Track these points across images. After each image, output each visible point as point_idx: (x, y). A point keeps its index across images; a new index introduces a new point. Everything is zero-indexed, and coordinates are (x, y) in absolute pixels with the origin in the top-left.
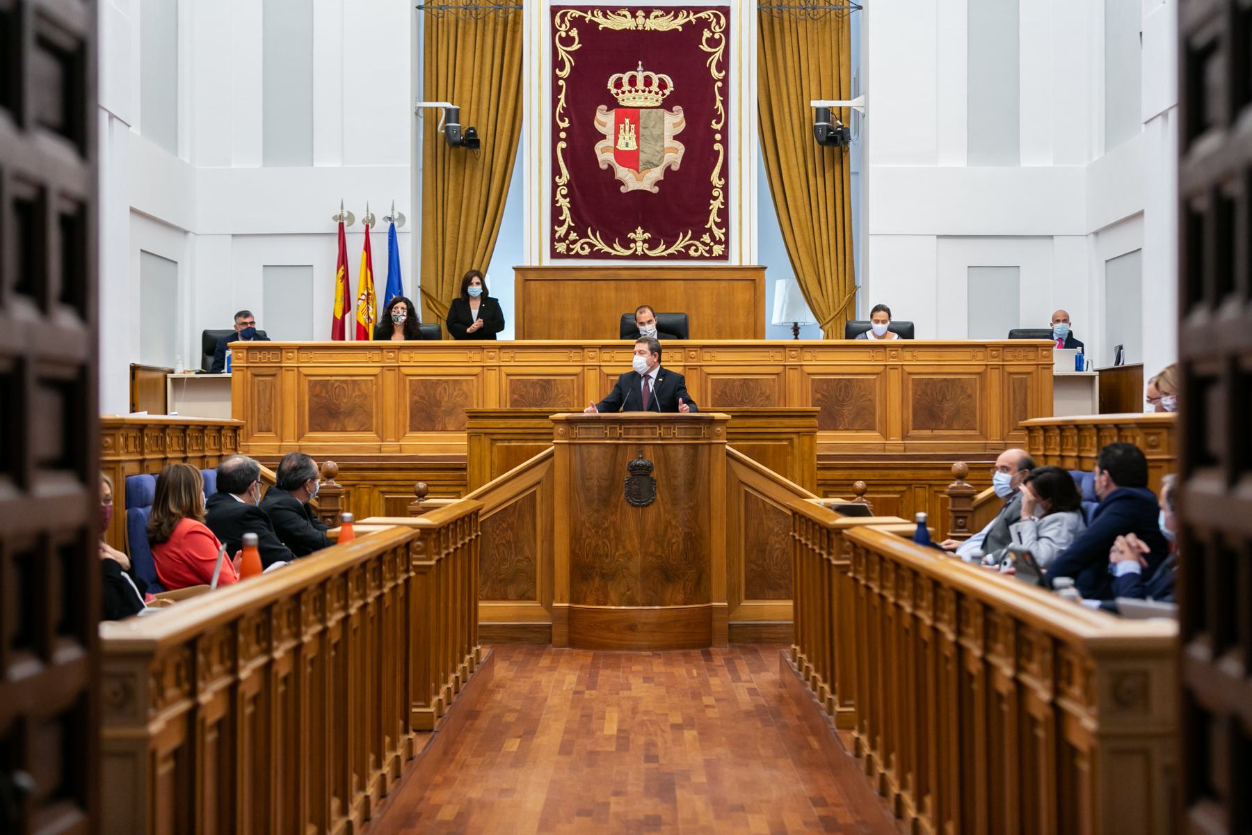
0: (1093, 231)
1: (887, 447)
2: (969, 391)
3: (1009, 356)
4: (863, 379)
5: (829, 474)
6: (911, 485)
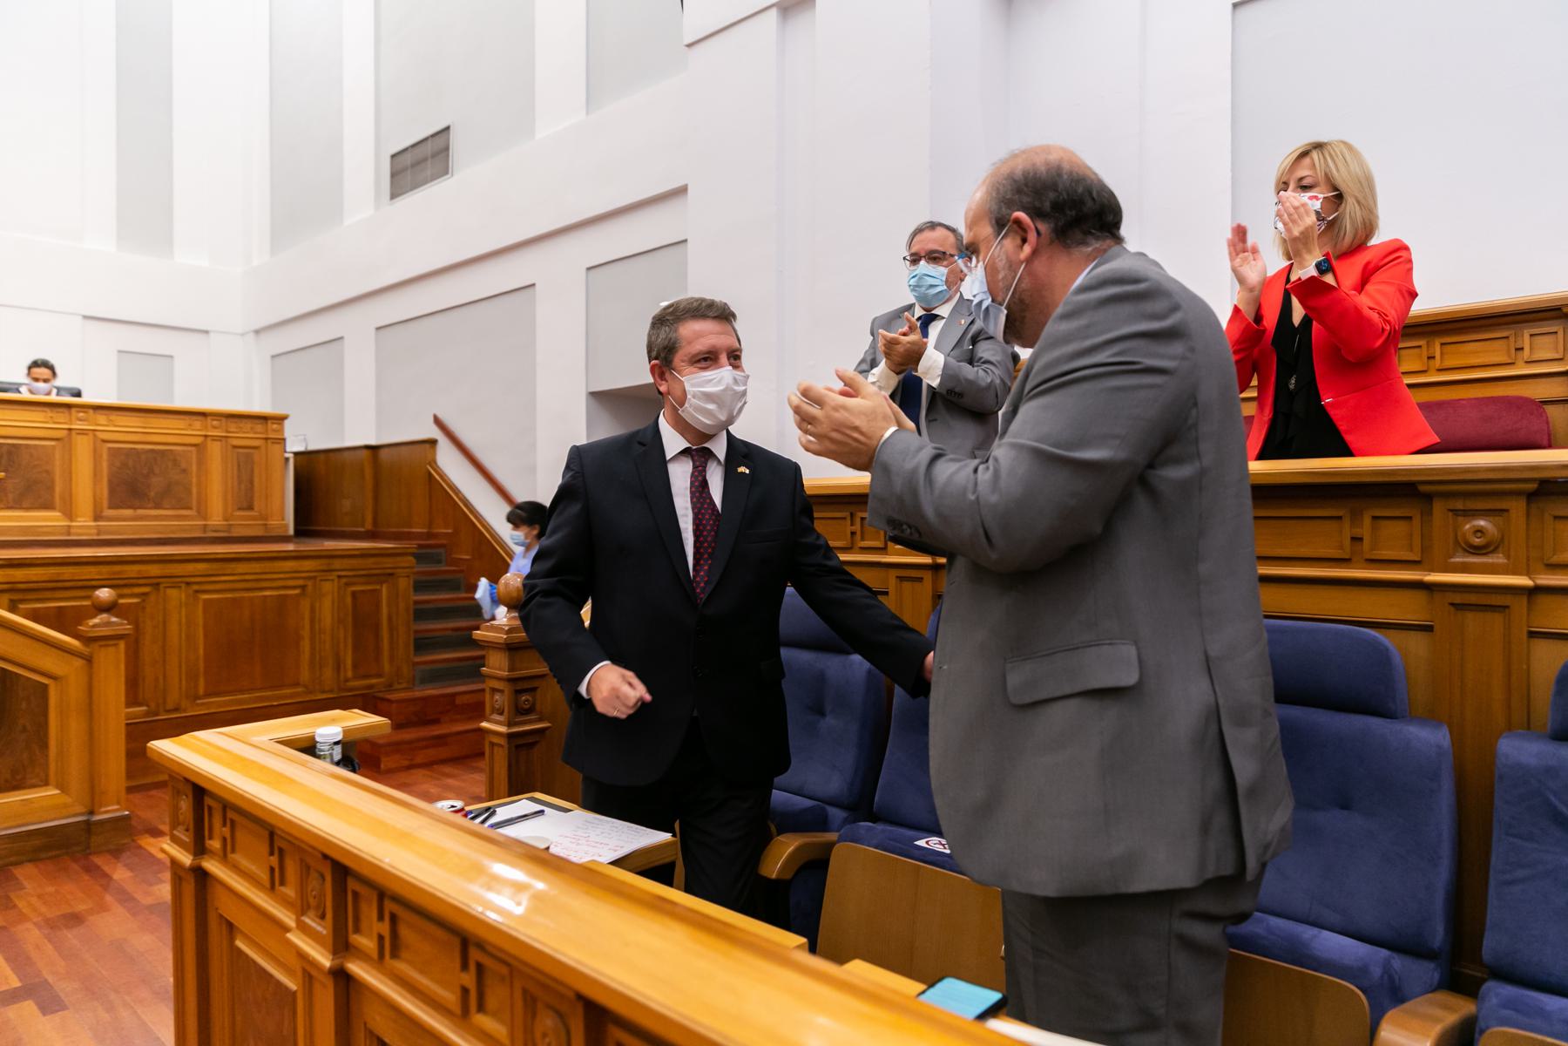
0: (257, 326)
1: (72, 531)
2: (183, 465)
3: (233, 426)
4: (35, 445)
5: (19, 574)
6: (158, 584)
